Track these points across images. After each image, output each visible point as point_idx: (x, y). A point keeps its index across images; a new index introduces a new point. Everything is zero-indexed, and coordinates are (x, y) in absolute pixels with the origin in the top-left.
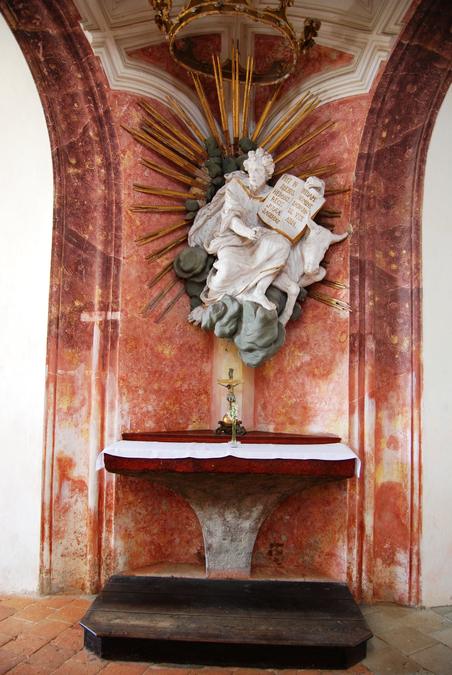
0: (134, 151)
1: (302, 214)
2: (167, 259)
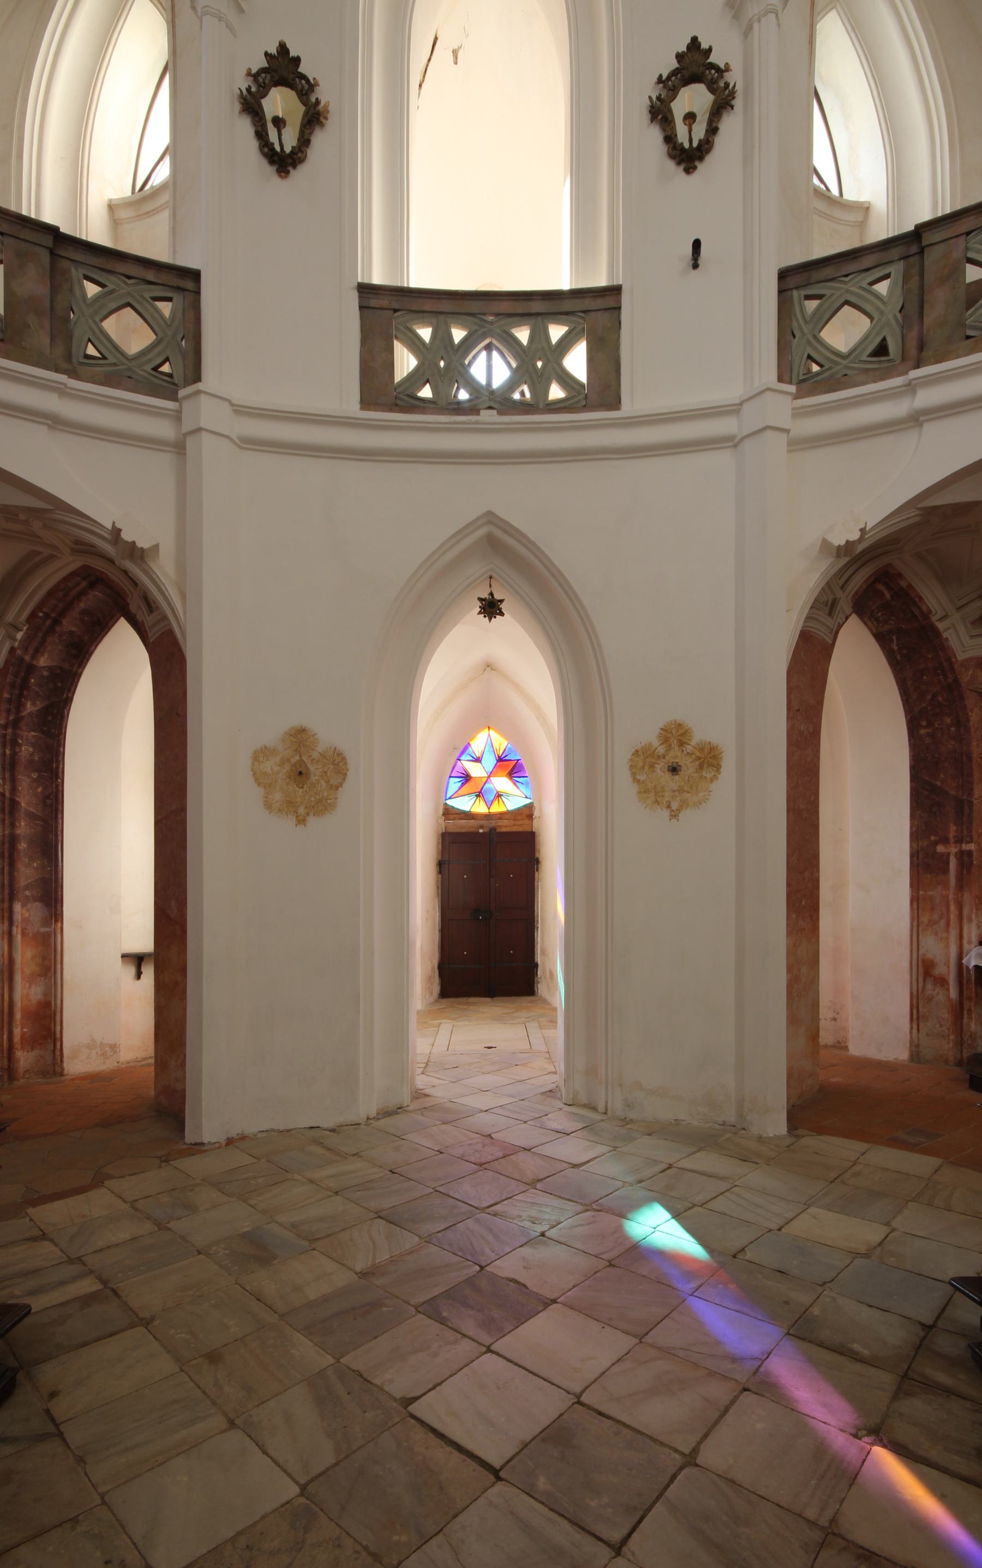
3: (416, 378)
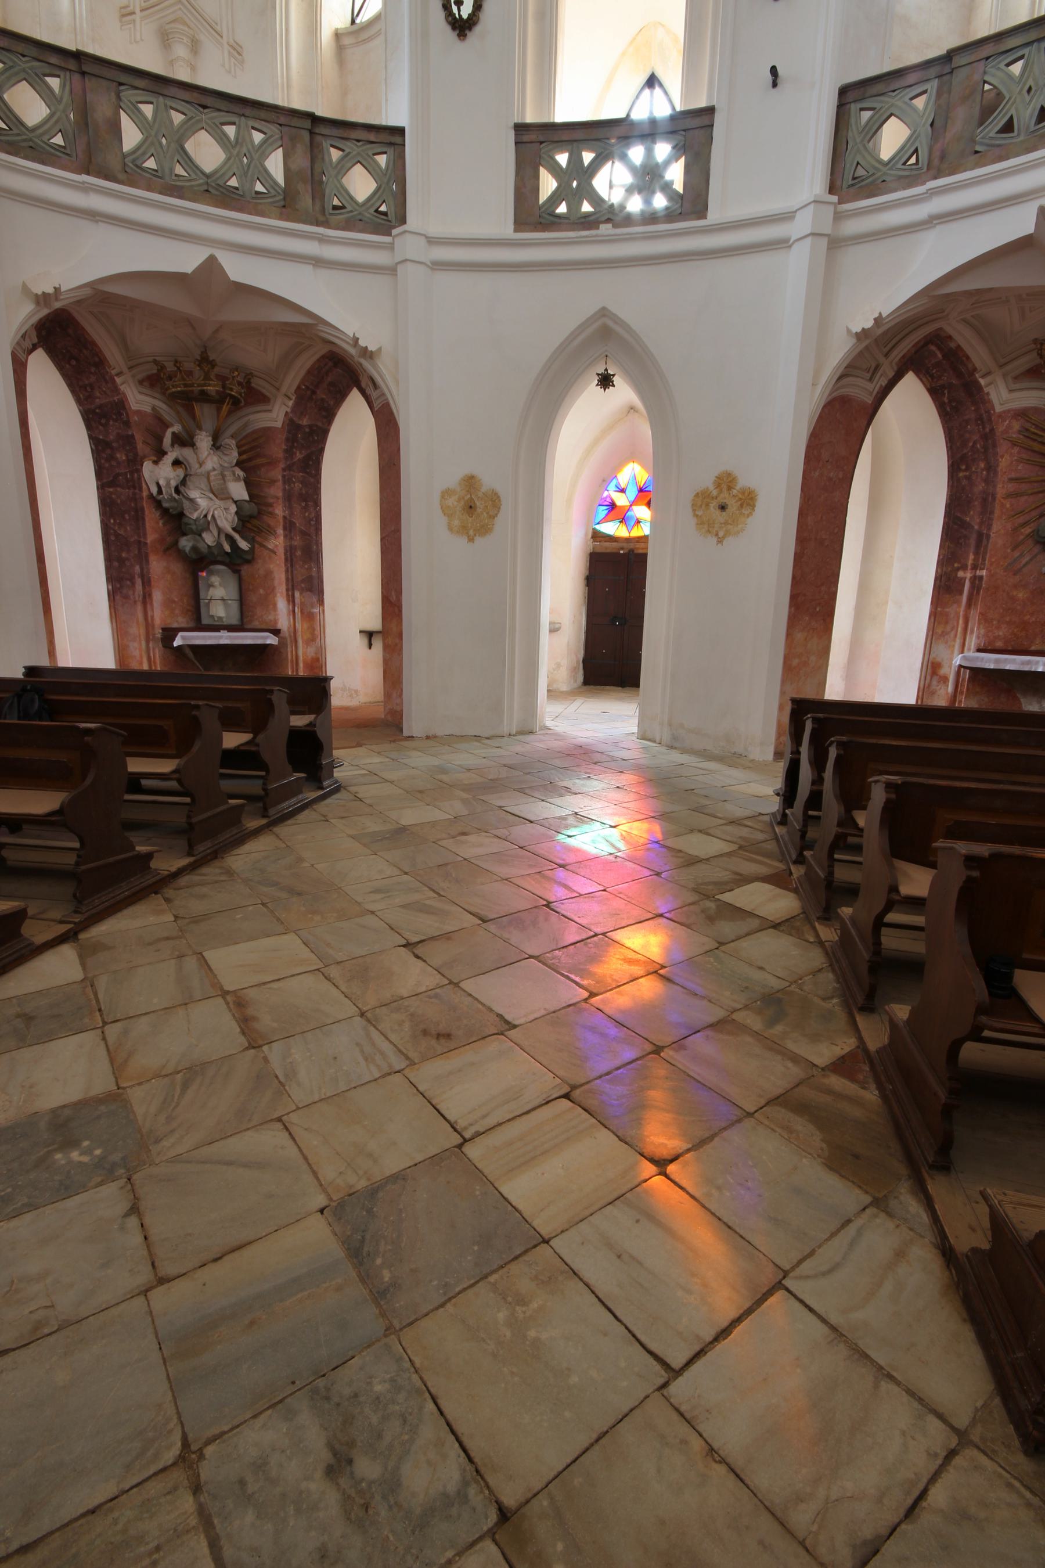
2: (1030, 528)
3: (555, 198)
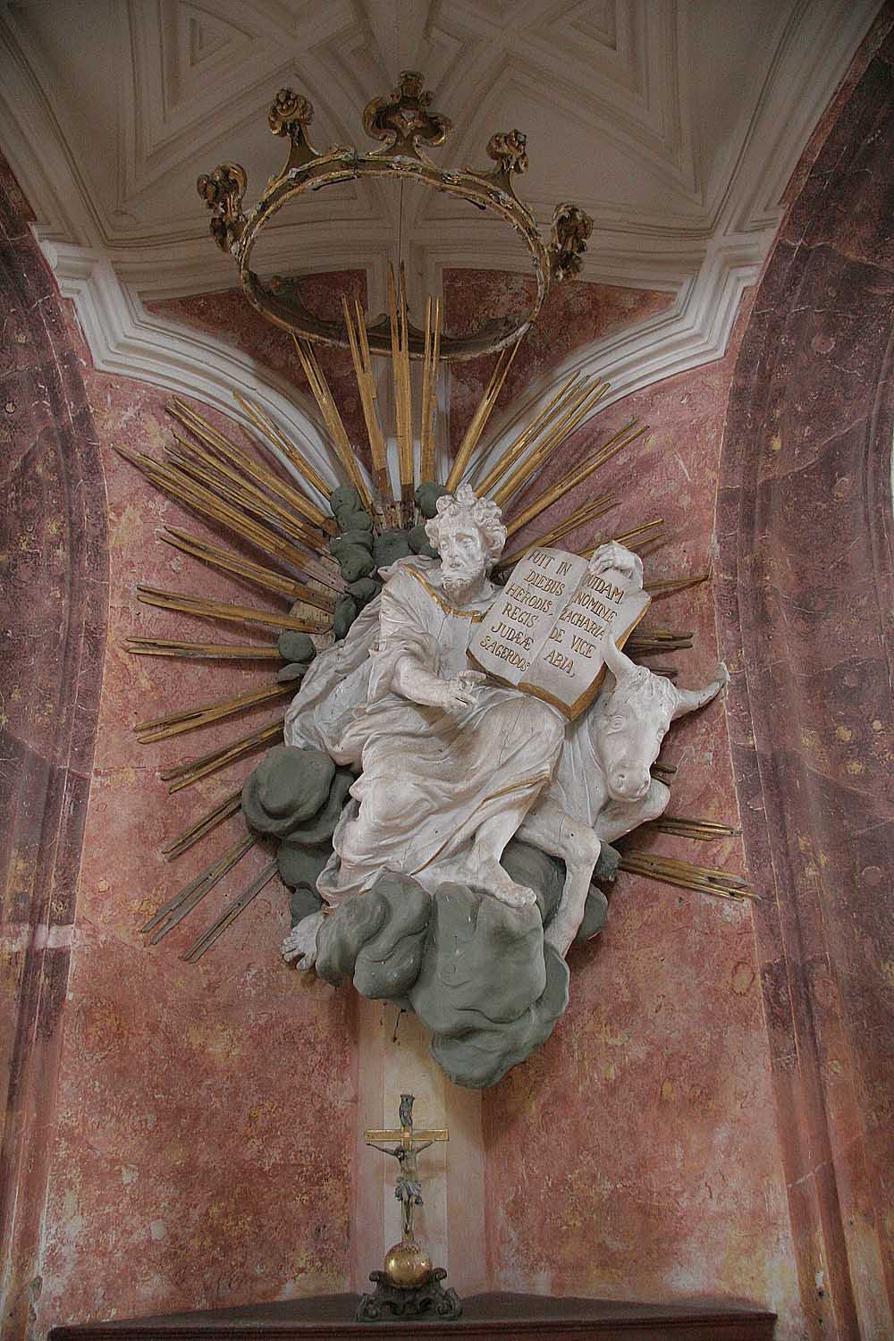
0: (147, 511)
1: (588, 637)
2: (225, 783)
